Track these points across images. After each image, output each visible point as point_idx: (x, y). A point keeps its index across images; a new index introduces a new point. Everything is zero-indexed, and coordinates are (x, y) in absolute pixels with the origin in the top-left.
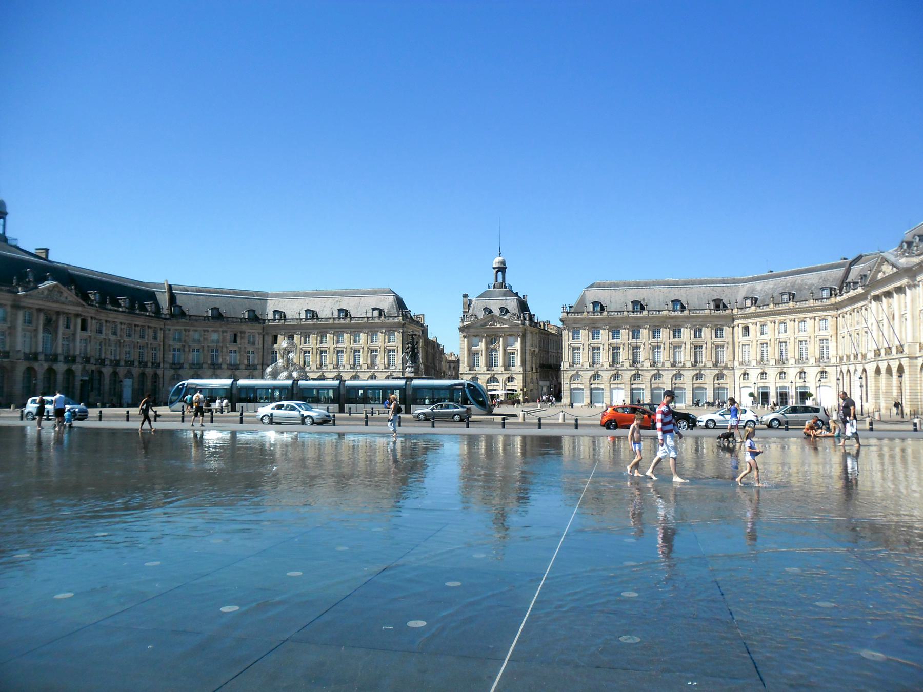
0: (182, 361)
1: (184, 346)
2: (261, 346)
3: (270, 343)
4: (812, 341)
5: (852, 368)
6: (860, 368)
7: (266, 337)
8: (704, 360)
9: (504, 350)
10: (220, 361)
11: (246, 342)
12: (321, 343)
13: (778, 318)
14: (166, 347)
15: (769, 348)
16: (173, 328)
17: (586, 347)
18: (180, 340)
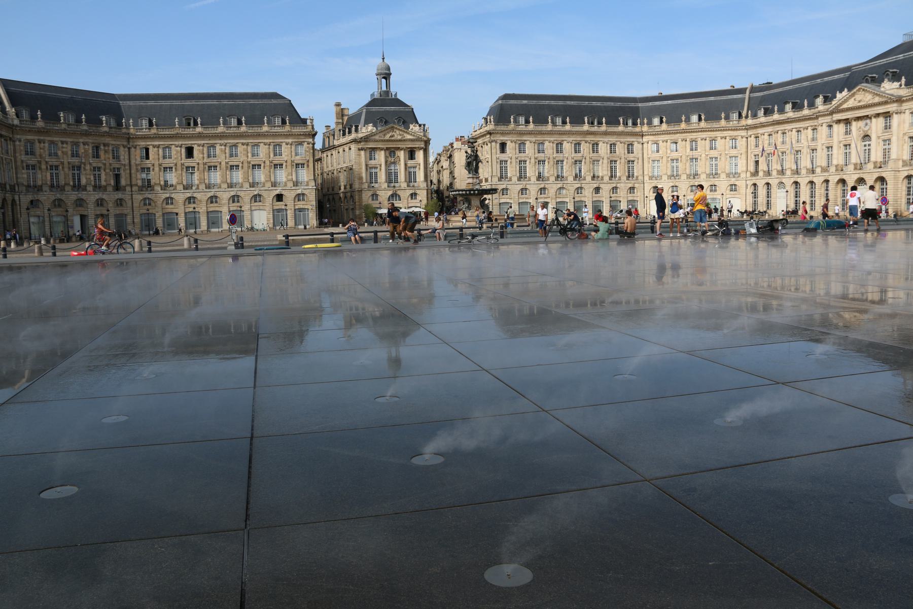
0: (39, 183)
1: (40, 162)
2: (127, 161)
3: (139, 159)
4: (723, 158)
5: (774, 182)
6: (788, 181)
7: (133, 150)
8: (618, 174)
9: (406, 165)
10: (84, 181)
11: (111, 156)
12: (209, 156)
13: (689, 136)
14: (19, 163)
15: (680, 164)
16: (24, 137)
17: (514, 160)
18: (32, 153)
